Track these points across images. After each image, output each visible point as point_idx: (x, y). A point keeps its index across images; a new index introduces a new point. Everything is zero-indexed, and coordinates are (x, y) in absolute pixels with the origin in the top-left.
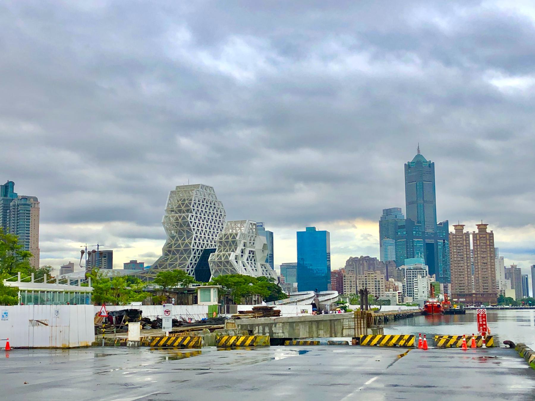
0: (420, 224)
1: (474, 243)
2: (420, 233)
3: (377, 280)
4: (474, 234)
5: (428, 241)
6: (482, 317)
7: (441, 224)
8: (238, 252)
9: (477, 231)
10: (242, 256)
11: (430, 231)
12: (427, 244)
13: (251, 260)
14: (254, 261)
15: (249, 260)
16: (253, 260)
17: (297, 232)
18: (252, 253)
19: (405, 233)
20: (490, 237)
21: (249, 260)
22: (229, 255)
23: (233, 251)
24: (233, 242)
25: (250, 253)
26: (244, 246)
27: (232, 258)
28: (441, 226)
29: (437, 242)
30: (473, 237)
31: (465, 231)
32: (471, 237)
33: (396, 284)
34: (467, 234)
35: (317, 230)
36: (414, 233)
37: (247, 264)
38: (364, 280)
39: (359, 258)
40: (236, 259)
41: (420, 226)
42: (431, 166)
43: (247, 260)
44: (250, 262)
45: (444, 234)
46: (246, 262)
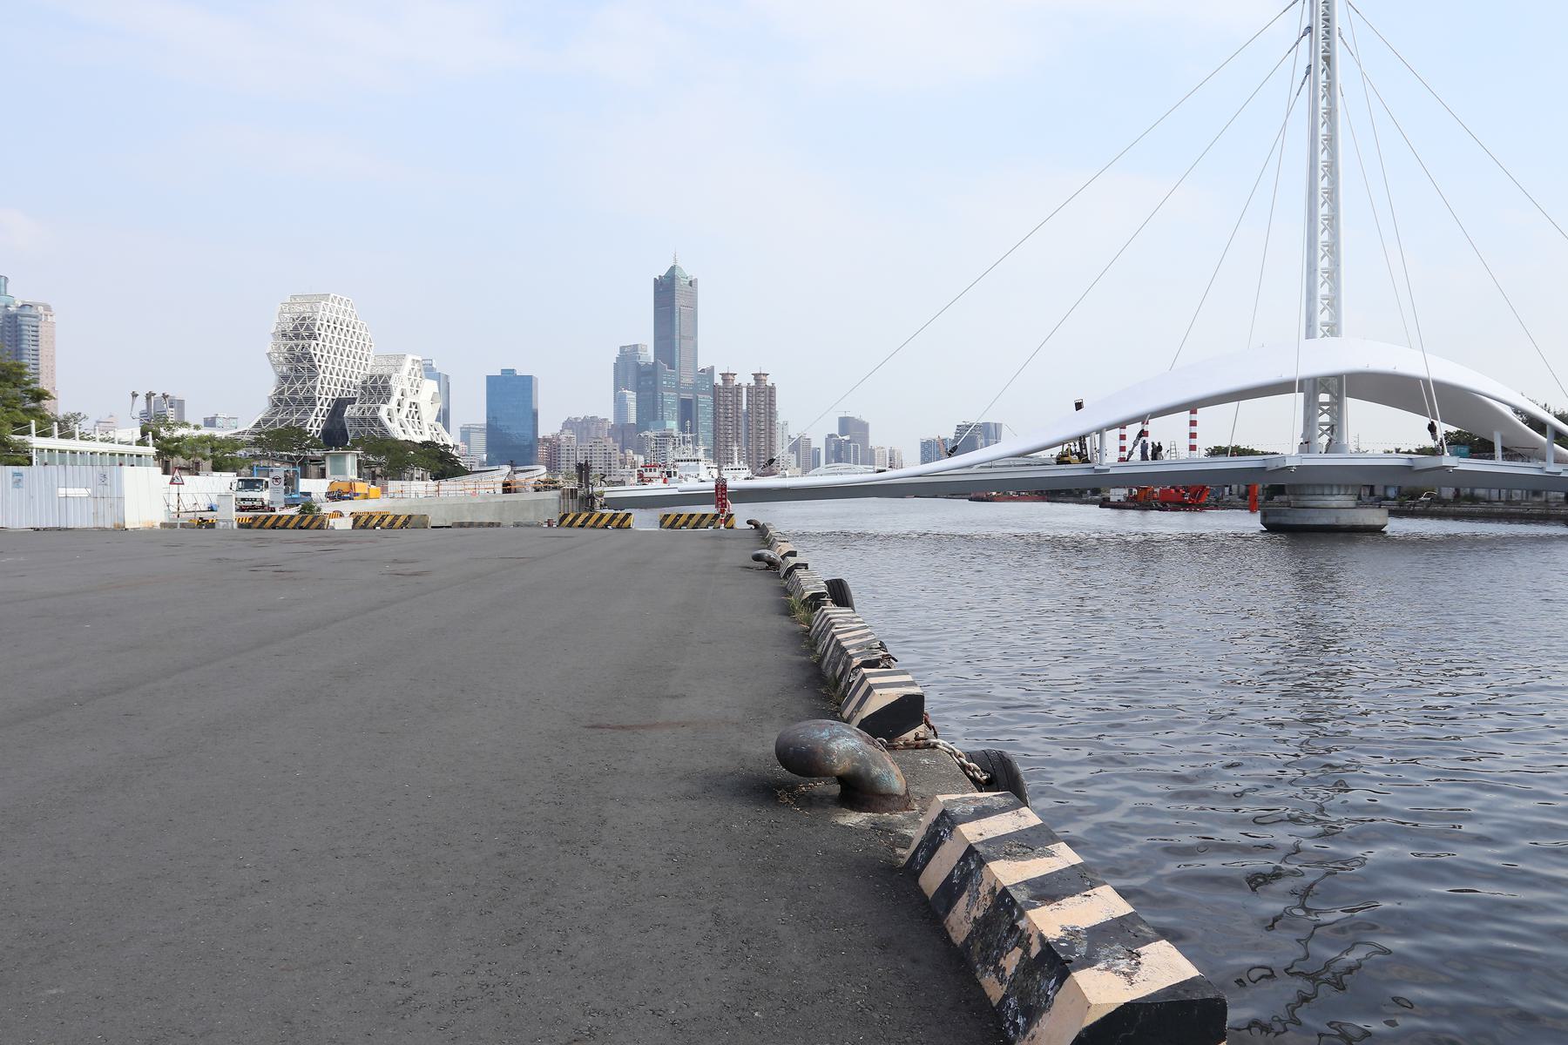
1: (748, 400)
2: (673, 384)
3: (607, 451)
6: (722, 489)
7: (703, 370)
8: (393, 404)
9: (753, 383)
10: (399, 410)
11: (687, 380)
13: (413, 418)
14: (418, 419)
15: (410, 417)
16: (416, 417)
17: (489, 378)
18: (414, 407)
19: (650, 383)
20: (770, 392)
21: (410, 417)
22: (378, 409)
23: (384, 403)
24: (384, 388)
25: (411, 407)
26: (402, 395)
27: (383, 414)
30: (748, 392)
31: (736, 383)
32: (745, 390)
33: (636, 459)
34: (739, 387)
36: (665, 383)
37: (406, 423)
38: (588, 452)
40: (389, 415)
41: (672, 373)
43: (407, 417)
44: (410, 419)
45: (707, 386)
46: (405, 420)
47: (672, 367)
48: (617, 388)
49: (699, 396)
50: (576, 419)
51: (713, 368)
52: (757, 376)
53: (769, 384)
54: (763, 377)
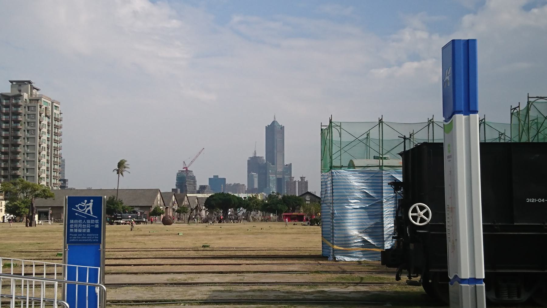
0: (274, 165)
4: (299, 182)
5: (278, 176)
7: (287, 165)
9: (300, 180)
12: (278, 178)
20: (306, 183)
28: (287, 167)
29: (284, 177)
30: (298, 183)
31: (294, 180)
32: (297, 183)
34: (295, 182)
35: (219, 177)
36: (270, 171)
39: (233, 184)
42: (282, 128)
45: (289, 172)
47: (273, 164)
48: (249, 172)
49: (286, 176)
50: (230, 184)
51: (291, 164)
52: (301, 178)
53: (306, 181)
54: (304, 178)
